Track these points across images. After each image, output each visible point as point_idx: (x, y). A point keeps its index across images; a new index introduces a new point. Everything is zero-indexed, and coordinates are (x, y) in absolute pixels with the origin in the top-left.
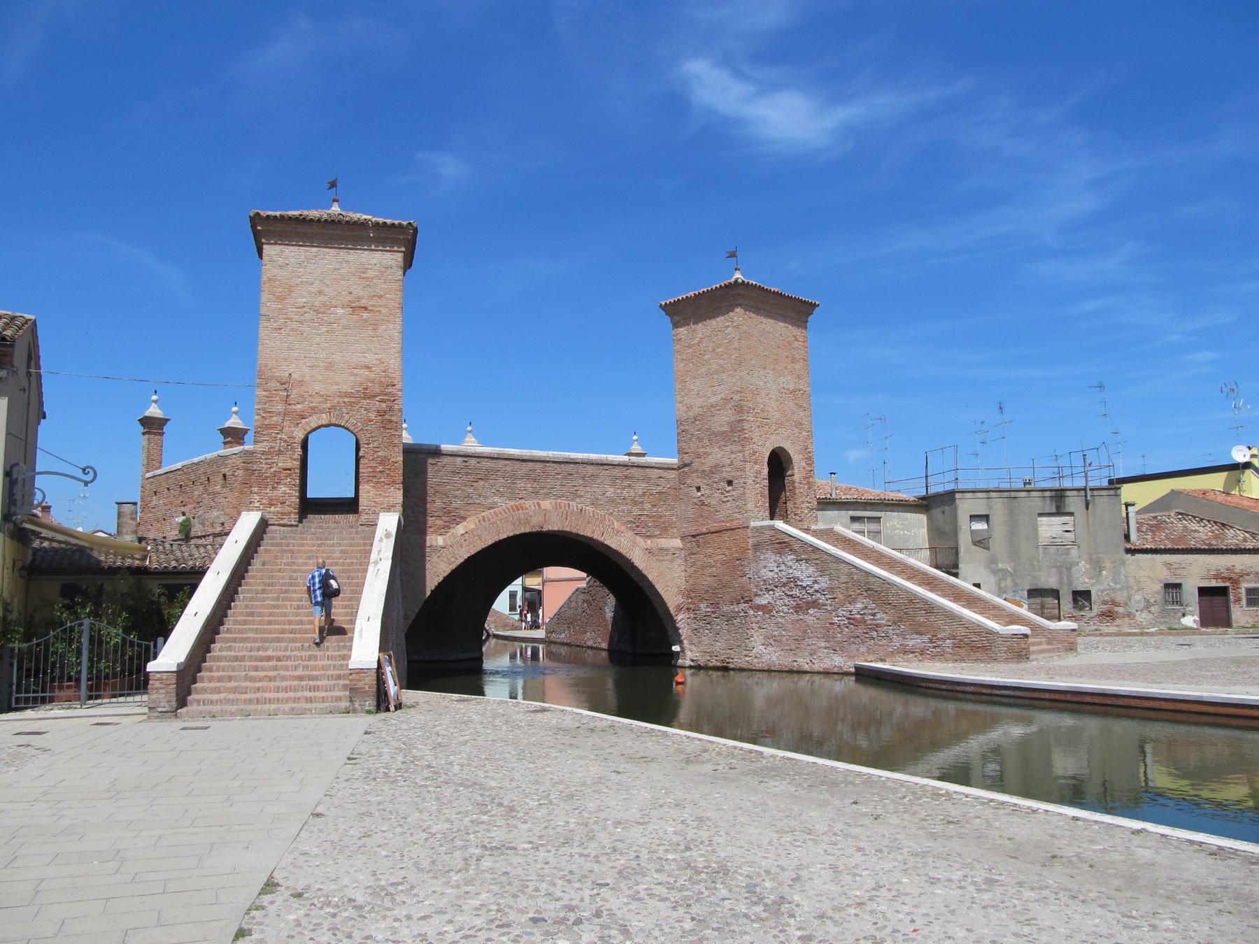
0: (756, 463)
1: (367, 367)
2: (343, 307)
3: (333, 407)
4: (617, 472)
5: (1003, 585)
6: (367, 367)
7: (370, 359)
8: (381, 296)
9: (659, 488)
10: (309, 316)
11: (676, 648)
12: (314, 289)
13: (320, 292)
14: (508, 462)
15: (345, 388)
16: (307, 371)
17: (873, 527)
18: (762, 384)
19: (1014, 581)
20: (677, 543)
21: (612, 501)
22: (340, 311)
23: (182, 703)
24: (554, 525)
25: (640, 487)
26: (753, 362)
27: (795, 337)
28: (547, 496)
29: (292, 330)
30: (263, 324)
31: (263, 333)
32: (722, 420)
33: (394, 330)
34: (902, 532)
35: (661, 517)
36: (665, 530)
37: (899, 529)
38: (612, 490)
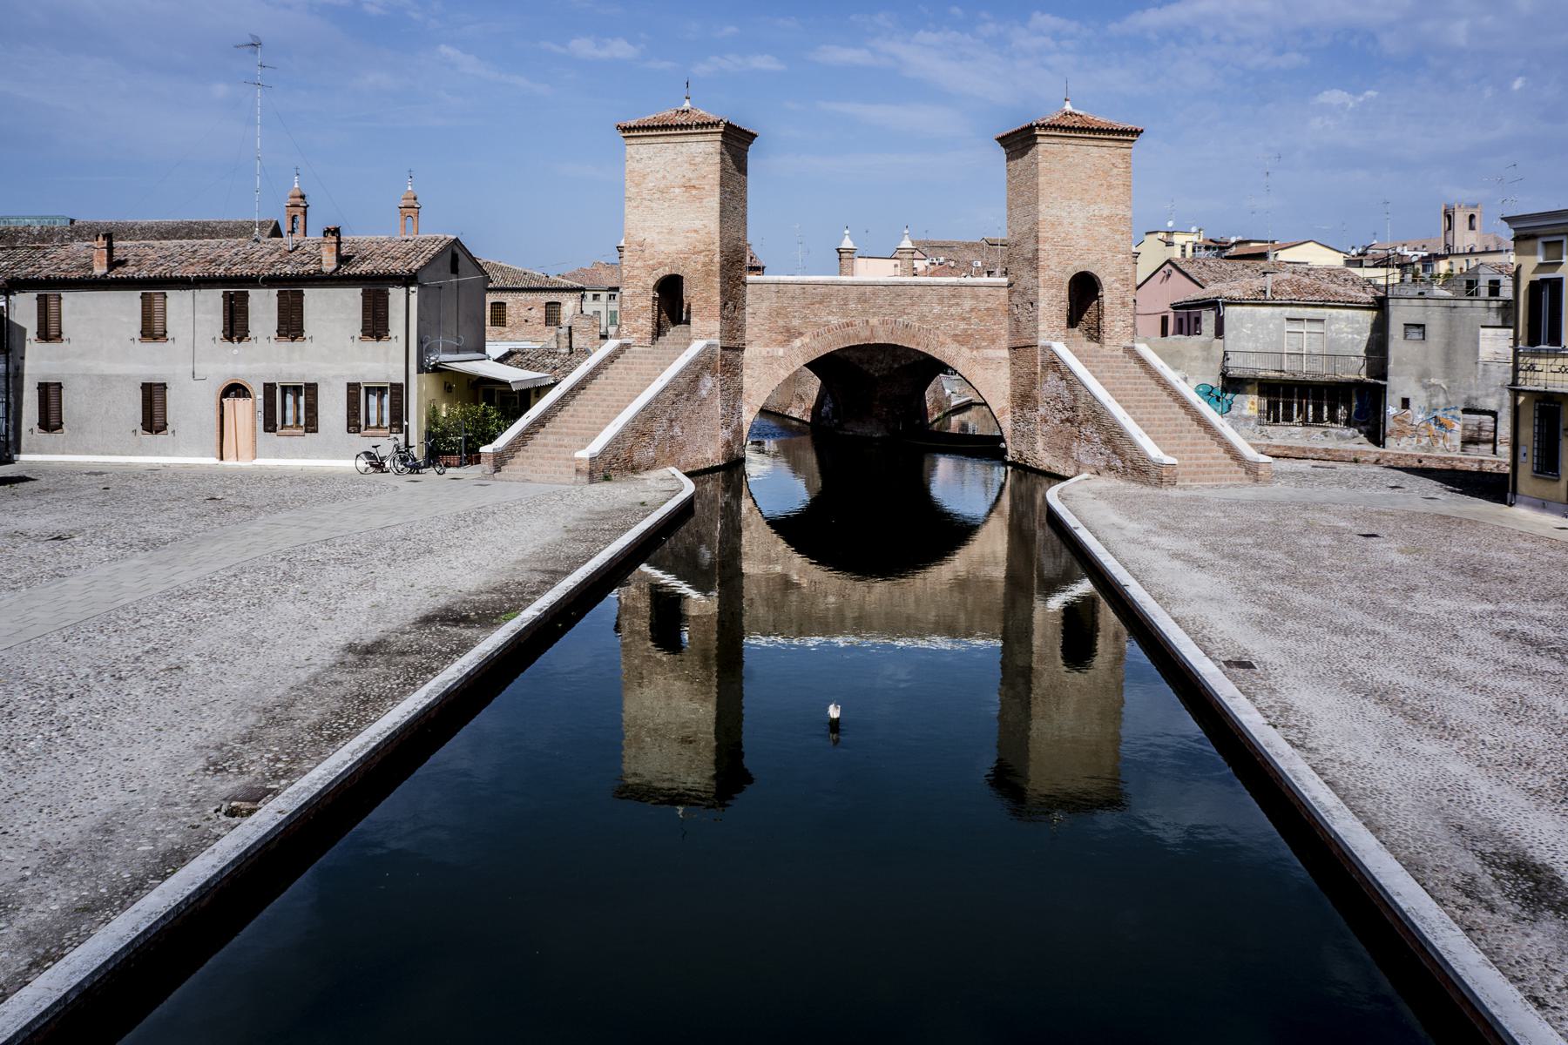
0: (1052, 288)
1: (696, 231)
2: (679, 187)
3: (673, 262)
4: (946, 292)
5: (1434, 402)
6: (696, 231)
7: (698, 224)
8: (704, 177)
9: (988, 305)
10: (656, 196)
11: (1003, 445)
12: (659, 176)
13: (664, 177)
14: (840, 287)
15: (680, 246)
16: (655, 236)
17: (1316, 327)
18: (1064, 214)
19: (1447, 399)
20: (1005, 353)
21: (939, 317)
22: (677, 190)
23: (498, 469)
24: (882, 338)
25: (968, 304)
26: (1054, 195)
27: (1113, 164)
28: (874, 314)
29: (646, 207)
30: (627, 204)
31: (627, 211)
32: (1028, 248)
33: (713, 202)
34: (1350, 336)
35: (988, 330)
36: (993, 341)
37: (1348, 333)
38: (939, 307)
